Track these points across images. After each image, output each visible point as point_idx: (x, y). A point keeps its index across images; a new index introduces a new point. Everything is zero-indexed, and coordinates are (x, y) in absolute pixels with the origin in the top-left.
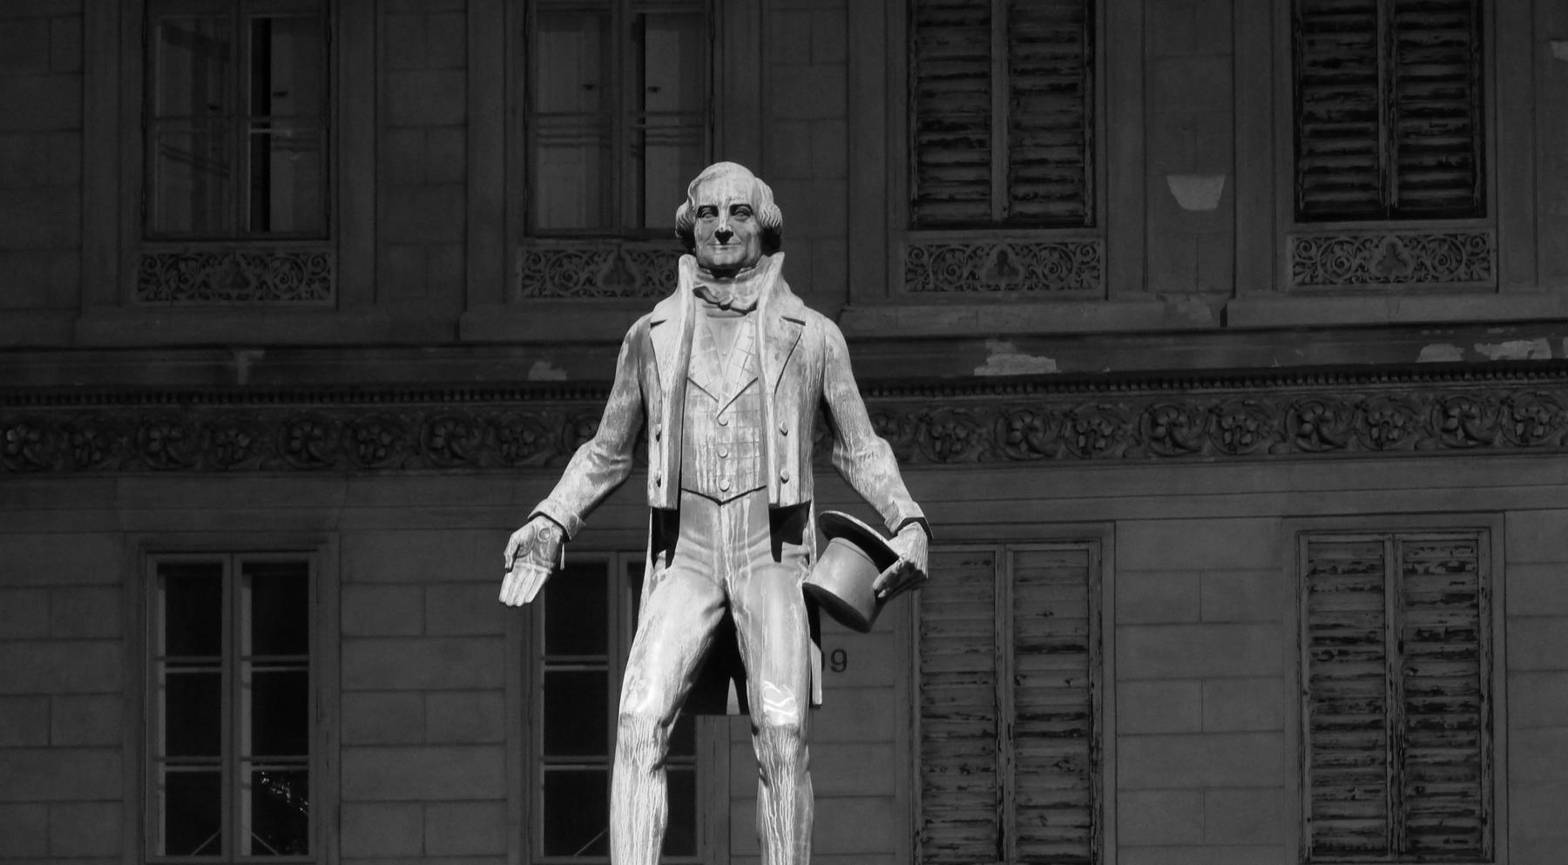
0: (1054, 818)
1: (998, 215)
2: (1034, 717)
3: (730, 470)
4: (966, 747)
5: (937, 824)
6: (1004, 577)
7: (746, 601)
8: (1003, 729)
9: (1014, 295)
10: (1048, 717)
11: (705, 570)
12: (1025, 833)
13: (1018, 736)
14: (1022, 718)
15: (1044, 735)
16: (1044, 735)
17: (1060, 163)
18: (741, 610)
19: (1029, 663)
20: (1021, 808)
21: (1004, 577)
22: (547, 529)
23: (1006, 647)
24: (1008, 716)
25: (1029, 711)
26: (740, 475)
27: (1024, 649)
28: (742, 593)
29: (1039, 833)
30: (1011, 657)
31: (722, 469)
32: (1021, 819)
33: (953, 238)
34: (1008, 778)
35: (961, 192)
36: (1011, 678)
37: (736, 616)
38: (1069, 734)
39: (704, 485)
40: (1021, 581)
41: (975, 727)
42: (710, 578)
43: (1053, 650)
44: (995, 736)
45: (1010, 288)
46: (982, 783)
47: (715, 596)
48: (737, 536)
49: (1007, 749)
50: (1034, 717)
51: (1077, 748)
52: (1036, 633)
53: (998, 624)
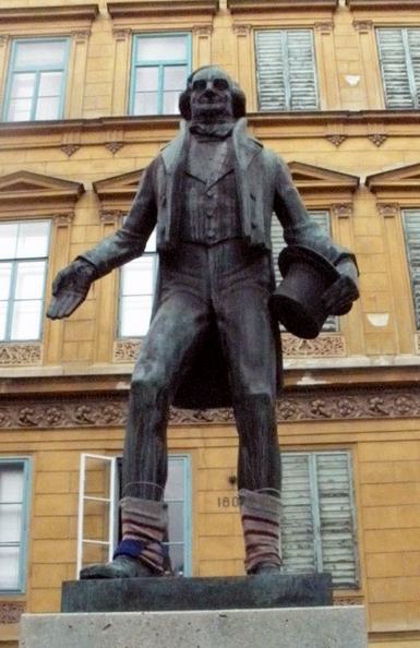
0: (339, 566)
2: (329, 524)
3: (214, 224)
4: (301, 537)
6: (313, 466)
7: (227, 311)
8: (315, 529)
10: (333, 524)
11: (197, 293)
13: (322, 533)
14: (323, 525)
16: (333, 531)
18: (223, 319)
19: (325, 501)
20: (325, 563)
21: (313, 466)
22: (82, 267)
23: (315, 494)
24: (317, 523)
25: (326, 521)
26: (223, 228)
27: (322, 495)
28: (224, 306)
30: (317, 497)
31: (209, 224)
36: (317, 507)
37: (220, 324)
38: (343, 531)
39: (196, 235)
40: (319, 468)
41: (305, 529)
42: (201, 300)
43: (335, 495)
45: (308, 354)
46: (308, 552)
47: (204, 310)
48: (220, 269)
49: (318, 537)
50: (329, 524)
51: (347, 536)
52: (327, 487)
53: (311, 484)
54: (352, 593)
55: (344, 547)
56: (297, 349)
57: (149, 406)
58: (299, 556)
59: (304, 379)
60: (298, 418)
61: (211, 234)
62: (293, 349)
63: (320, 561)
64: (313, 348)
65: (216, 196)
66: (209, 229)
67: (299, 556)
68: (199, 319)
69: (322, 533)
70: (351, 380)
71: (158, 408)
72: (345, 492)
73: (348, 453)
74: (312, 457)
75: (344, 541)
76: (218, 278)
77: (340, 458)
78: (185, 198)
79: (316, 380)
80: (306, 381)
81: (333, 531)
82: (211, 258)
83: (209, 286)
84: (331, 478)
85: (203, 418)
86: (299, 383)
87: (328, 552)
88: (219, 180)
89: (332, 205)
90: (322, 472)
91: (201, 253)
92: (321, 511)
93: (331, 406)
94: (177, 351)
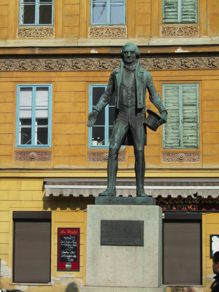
0: (190, 138)
2: (187, 118)
4: (173, 124)
6: (181, 91)
14: (184, 119)
16: (188, 122)
19: (185, 108)
21: (181, 91)
24: (181, 118)
27: (184, 105)
38: (193, 122)
43: (190, 105)
49: (181, 125)
51: (195, 124)
54: (195, 150)
55: (193, 129)
58: (172, 133)
59: (178, 49)
62: (174, 32)
63: (182, 136)
70: (200, 50)
72: (195, 104)
73: (198, 85)
75: (193, 126)
76: (131, 116)
77: (193, 87)
79: (184, 50)
80: (179, 50)
81: (188, 122)
82: (129, 110)
83: (128, 118)
84: (189, 97)
86: (176, 52)
90: (185, 94)
91: (126, 108)
92: (183, 113)
93: (190, 61)
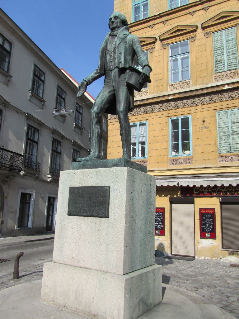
1: (226, 70)
3: (112, 64)
4: (225, 137)
5: (221, 147)
9: (228, 79)
12: (234, 147)
13: (232, 135)
15: (236, 134)
17: (234, 63)
19: (233, 125)
23: (230, 122)
24: (230, 132)
25: (233, 131)
26: (115, 64)
29: (236, 147)
32: (233, 145)
33: (220, 74)
34: (231, 140)
35: (221, 69)
36: (231, 127)
39: (109, 68)
40: (231, 115)
44: (229, 135)
47: (112, 88)
49: (231, 136)
52: (234, 121)
56: (224, 77)
57: (94, 118)
58: (225, 142)
59: (225, 87)
60: (224, 100)
61: (112, 67)
62: (223, 78)
63: (232, 143)
64: (229, 76)
65: (113, 55)
66: (111, 65)
67: (225, 142)
68: (110, 92)
69: (232, 135)
71: (96, 118)
74: (229, 111)
78: (105, 57)
80: (226, 87)
82: (112, 74)
84: (236, 117)
85: (194, 104)
86: (224, 89)
87: (234, 141)
88: (113, 50)
89: (236, 24)
90: (232, 116)
92: (232, 128)
94: (102, 102)
